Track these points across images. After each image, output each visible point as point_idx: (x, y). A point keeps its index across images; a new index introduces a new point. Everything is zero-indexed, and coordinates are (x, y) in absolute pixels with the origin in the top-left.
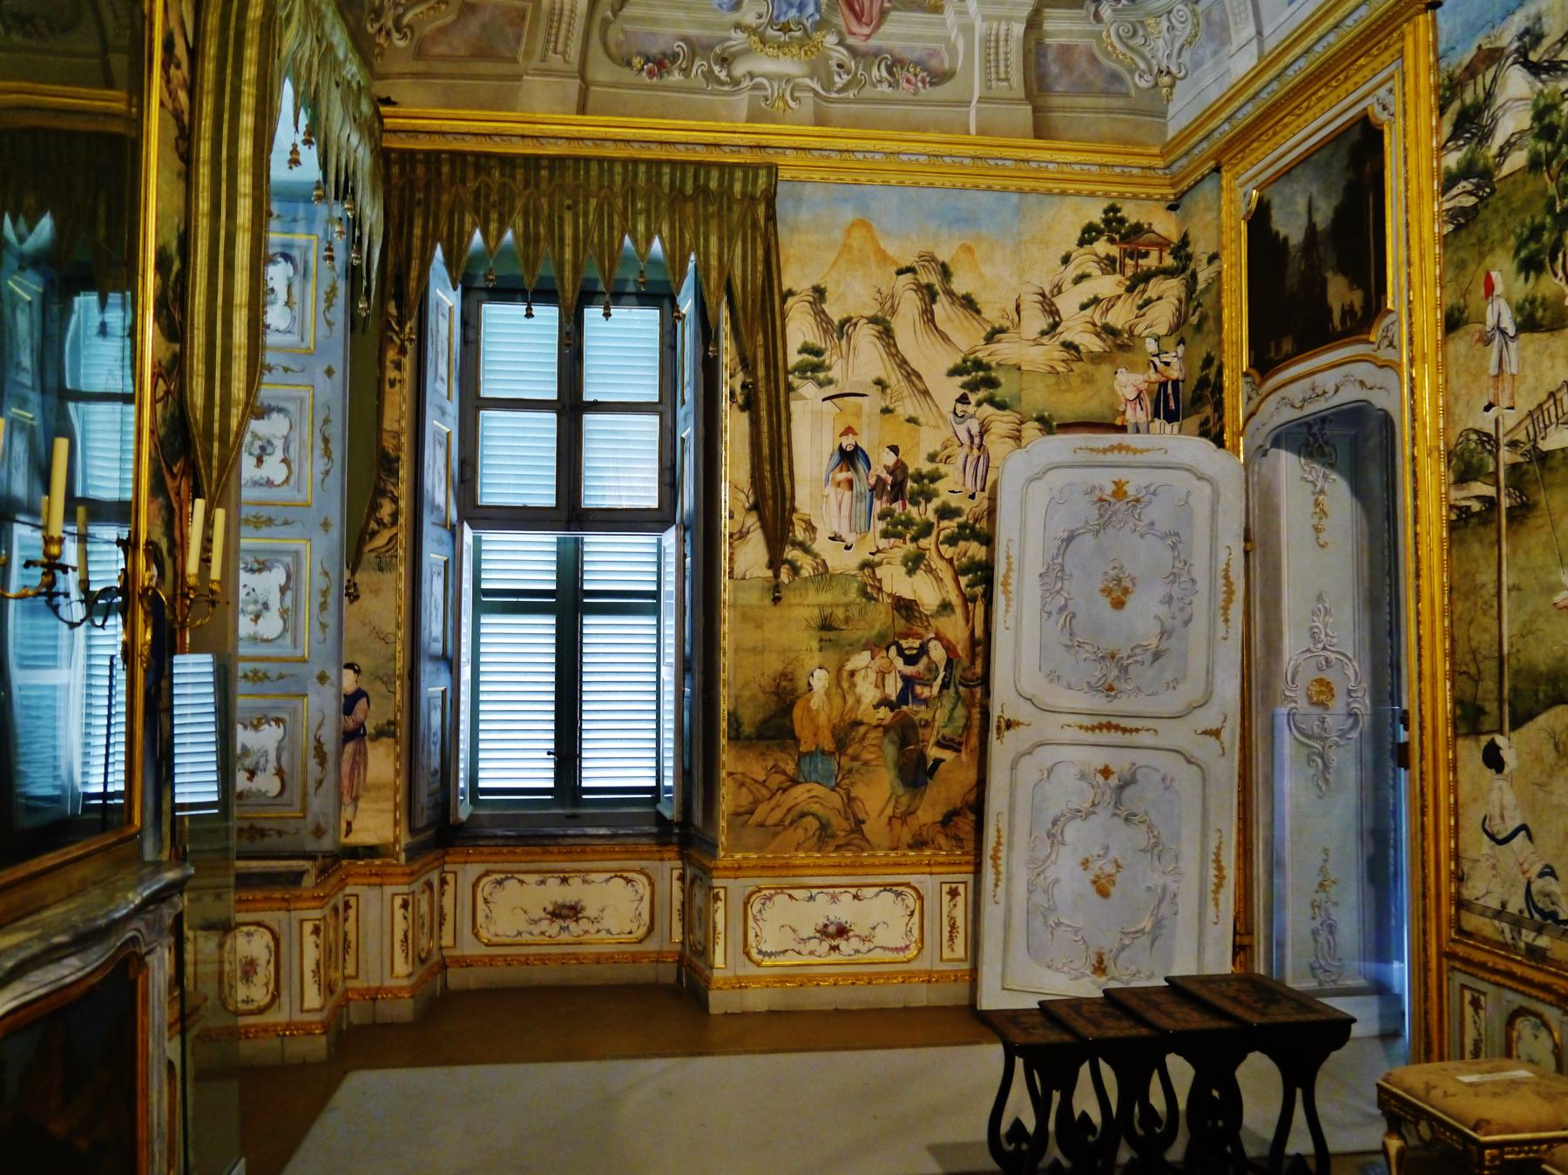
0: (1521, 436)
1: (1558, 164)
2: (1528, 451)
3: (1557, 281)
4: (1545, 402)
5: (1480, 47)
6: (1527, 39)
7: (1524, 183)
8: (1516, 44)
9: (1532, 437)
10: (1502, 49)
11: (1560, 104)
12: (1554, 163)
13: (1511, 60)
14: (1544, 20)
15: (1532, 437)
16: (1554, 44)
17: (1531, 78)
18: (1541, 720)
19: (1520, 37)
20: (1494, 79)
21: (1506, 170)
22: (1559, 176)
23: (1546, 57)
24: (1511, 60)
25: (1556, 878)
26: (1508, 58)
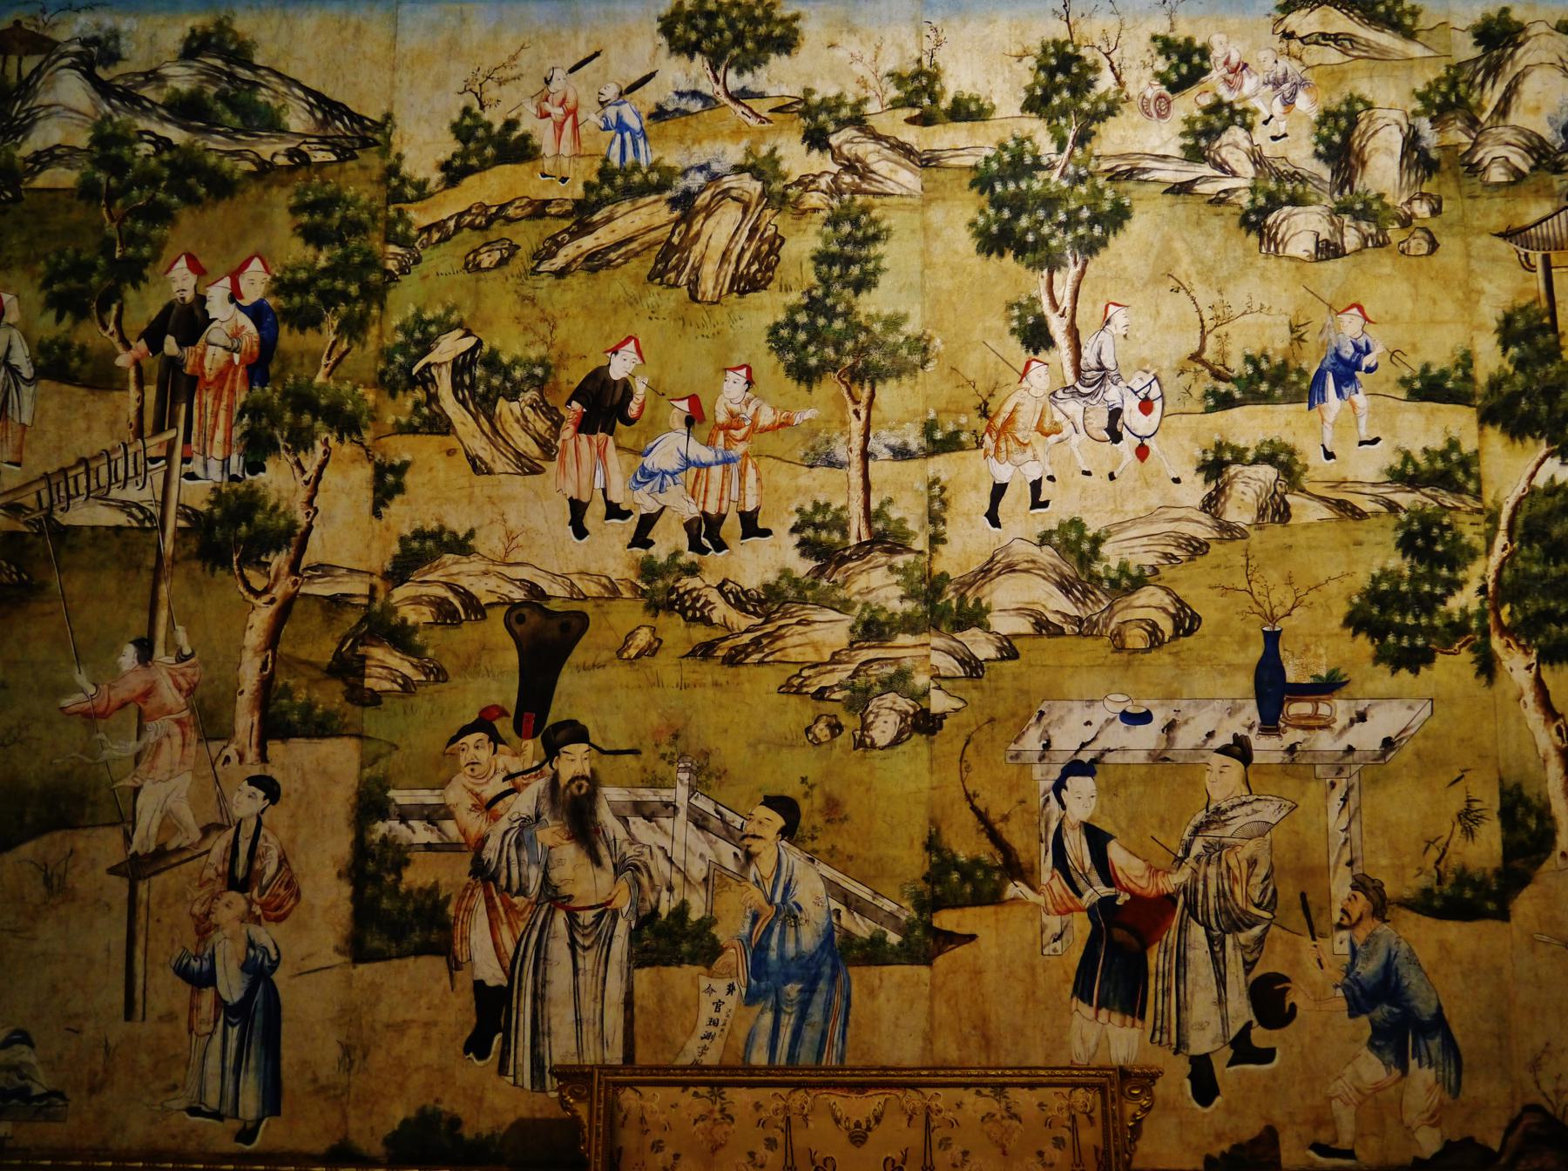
0: (29, 500)
1: (124, 206)
2: (39, 521)
3: (106, 334)
4: (71, 468)
5: (17, 23)
6: (95, 50)
7: (69, 209)
8: (75, 48)
9: (45, 504)
10: (57, 43)
11: (134, 142)
12: (119, 203)
13: (67, 61)
14: (123, 41)
15: (45, 504)
16: (136, 74)
17: (97, 96)
18: (26, 850)
19: (85, 43)
20: (37, 71)
21: (41, 181)
22: (123, 219)
23: (120, 82)
24: (67, 61)
25: (31, 1045)
26: (62, 56)
